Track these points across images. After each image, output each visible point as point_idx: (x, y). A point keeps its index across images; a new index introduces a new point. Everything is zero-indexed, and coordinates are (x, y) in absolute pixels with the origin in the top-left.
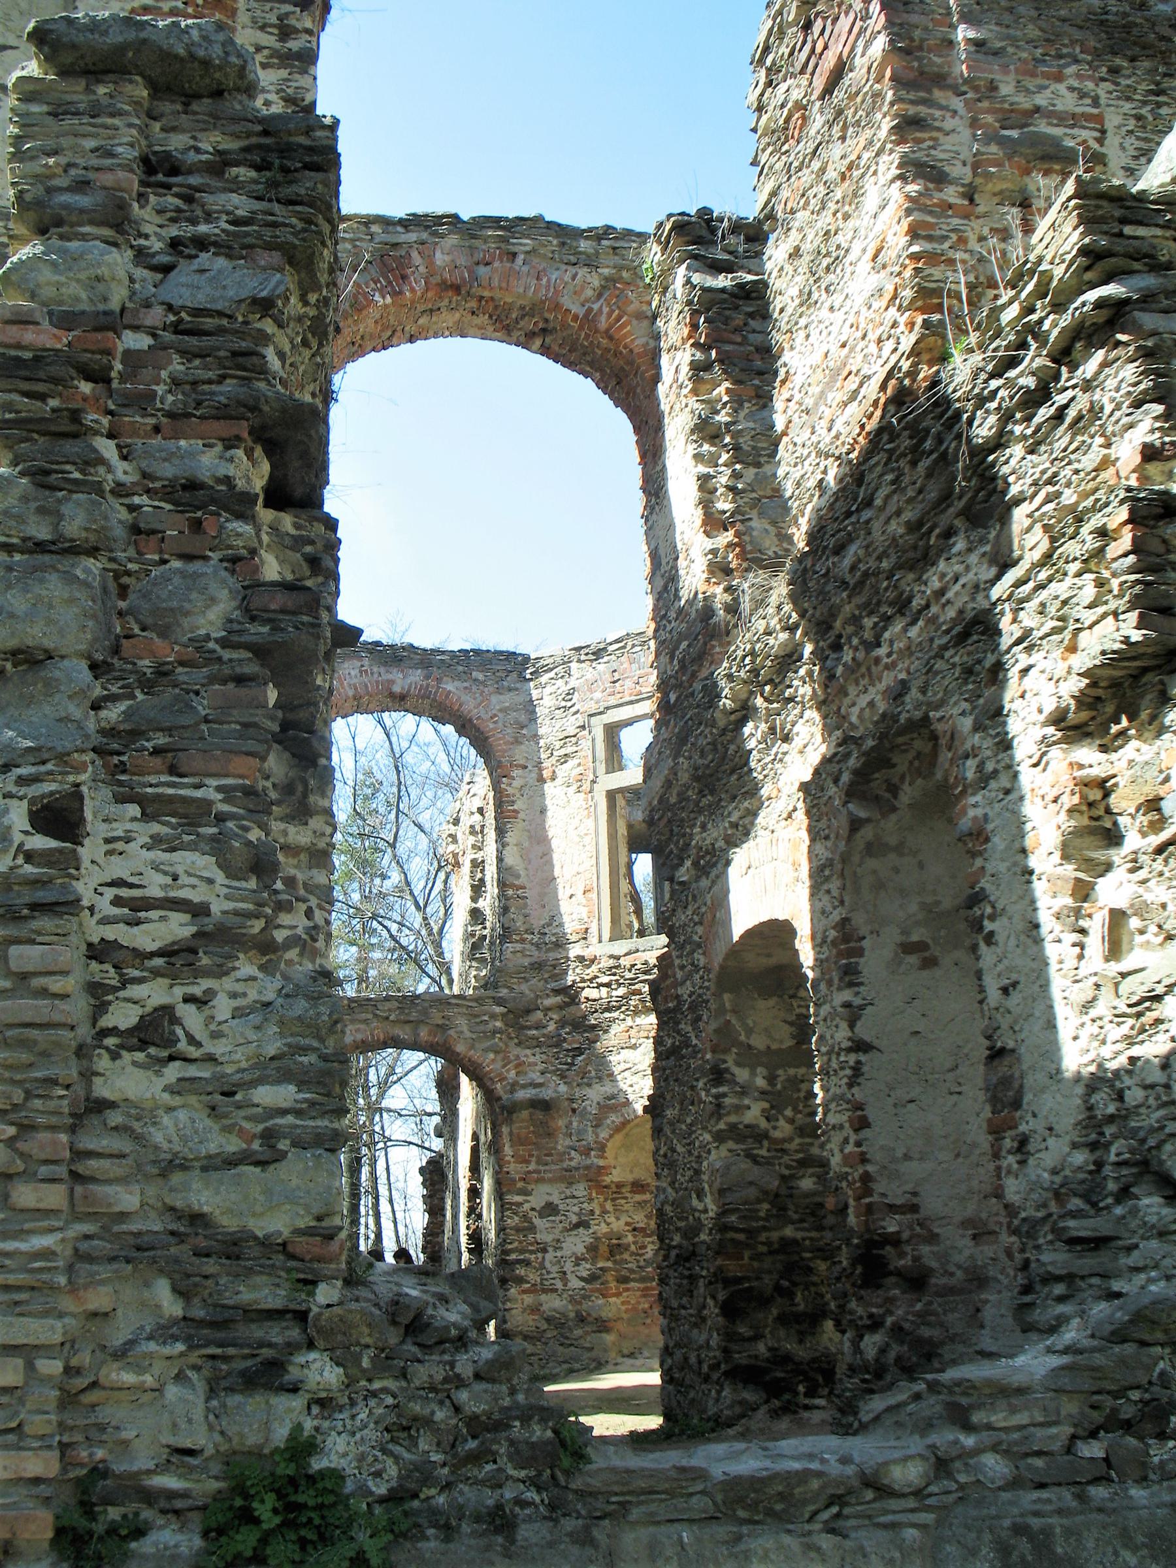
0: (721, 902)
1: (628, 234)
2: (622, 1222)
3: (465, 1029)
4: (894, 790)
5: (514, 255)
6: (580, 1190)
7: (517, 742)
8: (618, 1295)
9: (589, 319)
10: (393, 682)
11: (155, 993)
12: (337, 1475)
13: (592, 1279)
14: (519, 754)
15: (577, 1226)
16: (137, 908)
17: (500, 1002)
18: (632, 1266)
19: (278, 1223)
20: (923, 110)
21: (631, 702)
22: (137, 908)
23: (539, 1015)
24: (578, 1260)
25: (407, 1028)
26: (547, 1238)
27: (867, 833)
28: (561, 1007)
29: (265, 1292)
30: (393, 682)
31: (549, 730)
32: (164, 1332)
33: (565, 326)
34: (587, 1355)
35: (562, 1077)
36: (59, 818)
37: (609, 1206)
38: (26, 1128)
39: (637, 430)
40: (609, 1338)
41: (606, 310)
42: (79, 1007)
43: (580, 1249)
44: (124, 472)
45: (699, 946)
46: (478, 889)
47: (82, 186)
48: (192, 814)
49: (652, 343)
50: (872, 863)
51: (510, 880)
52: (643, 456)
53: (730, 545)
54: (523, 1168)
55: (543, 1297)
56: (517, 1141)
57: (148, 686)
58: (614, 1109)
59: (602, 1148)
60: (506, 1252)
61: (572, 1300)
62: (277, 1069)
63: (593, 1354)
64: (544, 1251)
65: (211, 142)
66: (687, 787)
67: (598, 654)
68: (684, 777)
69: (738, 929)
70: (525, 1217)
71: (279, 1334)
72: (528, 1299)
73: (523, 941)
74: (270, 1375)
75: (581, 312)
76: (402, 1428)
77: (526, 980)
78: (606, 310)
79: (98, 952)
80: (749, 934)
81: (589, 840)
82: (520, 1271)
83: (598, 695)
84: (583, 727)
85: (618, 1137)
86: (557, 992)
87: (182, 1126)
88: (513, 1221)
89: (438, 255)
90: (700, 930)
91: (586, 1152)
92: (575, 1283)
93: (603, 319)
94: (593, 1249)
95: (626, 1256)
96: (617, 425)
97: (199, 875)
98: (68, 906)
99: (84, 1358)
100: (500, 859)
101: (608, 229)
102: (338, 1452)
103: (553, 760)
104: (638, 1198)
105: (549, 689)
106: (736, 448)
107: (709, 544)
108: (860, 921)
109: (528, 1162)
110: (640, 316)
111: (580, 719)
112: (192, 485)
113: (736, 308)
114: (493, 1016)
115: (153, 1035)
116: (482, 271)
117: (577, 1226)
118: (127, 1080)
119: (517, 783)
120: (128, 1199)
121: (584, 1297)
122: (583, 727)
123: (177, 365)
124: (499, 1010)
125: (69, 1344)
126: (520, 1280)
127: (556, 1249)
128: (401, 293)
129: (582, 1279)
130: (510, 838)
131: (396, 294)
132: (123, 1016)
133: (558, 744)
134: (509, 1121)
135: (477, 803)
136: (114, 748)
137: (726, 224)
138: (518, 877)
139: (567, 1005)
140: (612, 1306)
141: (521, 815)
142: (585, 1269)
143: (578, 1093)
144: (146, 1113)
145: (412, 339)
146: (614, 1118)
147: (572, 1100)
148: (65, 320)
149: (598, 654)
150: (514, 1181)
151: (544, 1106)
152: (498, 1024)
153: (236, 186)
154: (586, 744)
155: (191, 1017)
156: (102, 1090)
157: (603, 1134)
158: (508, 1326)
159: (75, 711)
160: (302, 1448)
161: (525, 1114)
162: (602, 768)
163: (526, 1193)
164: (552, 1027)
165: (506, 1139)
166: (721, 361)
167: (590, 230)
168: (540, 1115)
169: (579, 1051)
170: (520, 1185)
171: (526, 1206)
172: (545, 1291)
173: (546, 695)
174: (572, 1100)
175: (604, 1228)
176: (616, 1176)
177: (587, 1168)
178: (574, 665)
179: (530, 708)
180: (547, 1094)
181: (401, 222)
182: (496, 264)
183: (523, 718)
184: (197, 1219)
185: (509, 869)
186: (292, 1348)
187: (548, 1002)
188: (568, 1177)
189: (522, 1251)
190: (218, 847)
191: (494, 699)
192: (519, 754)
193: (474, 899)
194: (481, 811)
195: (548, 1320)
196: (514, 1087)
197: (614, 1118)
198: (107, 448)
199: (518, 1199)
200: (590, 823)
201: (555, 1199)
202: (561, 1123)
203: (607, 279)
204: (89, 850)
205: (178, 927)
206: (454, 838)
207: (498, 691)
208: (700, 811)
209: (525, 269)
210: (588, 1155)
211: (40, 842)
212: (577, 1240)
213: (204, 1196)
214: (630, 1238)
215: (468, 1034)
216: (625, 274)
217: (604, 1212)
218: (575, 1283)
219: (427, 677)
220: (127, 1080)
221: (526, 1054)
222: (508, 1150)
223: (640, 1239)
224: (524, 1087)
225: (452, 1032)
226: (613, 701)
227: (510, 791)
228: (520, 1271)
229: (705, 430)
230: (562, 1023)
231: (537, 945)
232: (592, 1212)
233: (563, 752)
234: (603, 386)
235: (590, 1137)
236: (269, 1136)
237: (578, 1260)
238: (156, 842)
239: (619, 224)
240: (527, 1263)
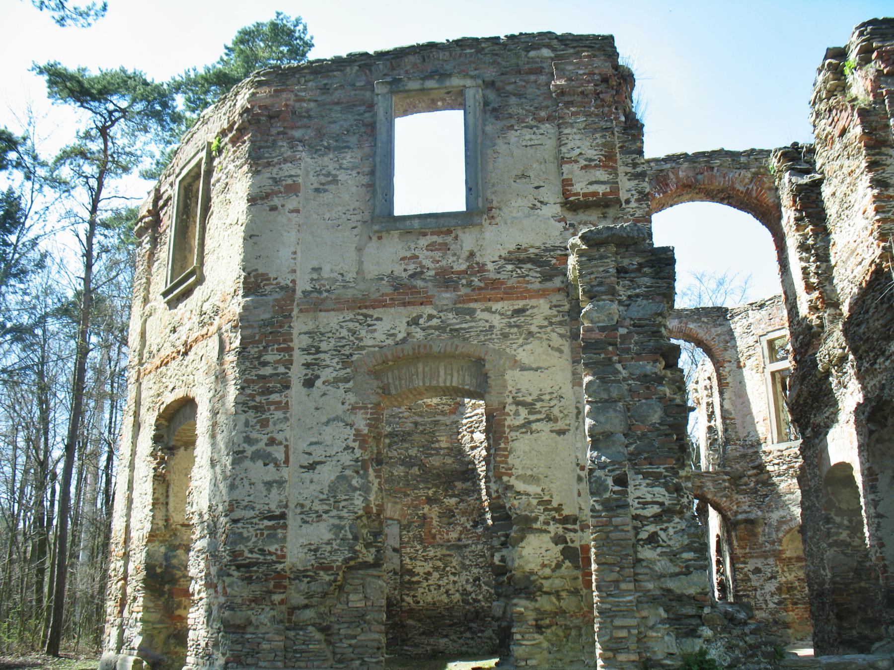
0: (825, 449)
1: (761, 151)
2: (793, 576)
4: (886, 419)
5: (713, 168)
6: (771, 561)
7: (726, 350)
8: (793, 611)
9: (748, 193)
11: (652, 528)
12: (714, 660)
13: (780, 603)
14: (727, 355)
15: (771, 578)
16: (644, 504)
17: (727, 474)
18: (799, 597)
19: (692, 591)
20: (878, 157)
21: (779, 329)
22: (644, 504)
23: (746, 479)
24: (772, 595)
26: (758, 584)
27: (876, 435)
28: (756, 475)
29: (689, 610)
31: (742, 344)
32: (663, 622)
33: (738, 196)
35: (759, 508)
36: (621, 481)
37: (786, 569)
38: (622, 568)
39: (774, 235)
40: (790, 631)
41: (755, 188)
42: (632, 534)
43: (773, 589)
44: (624, 373)
45: (816, 466)
46: (711, 416)
47: (601, 284)
48: (657, 476)
49: (777, 201)
50: (879, 446)
51: (728, 416)
52: (777, 247)
53: (817, 298)
54: (742, 551)
56: (739, 539)
57: (640, 439)
58: (785, 523)
59: (780, 541)
60: (738, 591)
61: (771, 613)
62: (688, 548)
64: (756, 590)
65: (636, 260)
66: (806, 398)
67: (761, 306)
68: (805, 394)
69: (832, 464)
70: (746, 575)
71: (694, 622)
73: (735, 444)
74: (693, 633)
75: (744, 190)
76: (730, 648)
77: (739, 463)
78: (755, 188)
79: (636, 517)
80: (835, 465)
81: (764, 395)
83: (763, 326)
84: (757, 342)
85: (788, 536)
86: (754, 468)
87: (663, 566)
88: (740, 576)
89: (680, 173)
90: (816, 460)
92: (771, 605)
93: (754, 192)
94: (779, 589)
95: (796, 592)
96: (765, 235)
97: (661, 494)
98: (626, 506)
99: (642, 629)
100: (722, 406)
101: (753, 150)
102: (713, 654)
103: (744, 358)
104: (800, 564)
105: (739, 324)
106: (817, 255)
107: (808, 297)
108: (876, 468)
110: (770, 189)
111: (755, 338)
112: (646, 376)
113: (812, 191)
114: (724, 481)
115: (653, 539)
116: (700, 177)
118: (647, 553)
119: (727, 370)
120: (650, 586)
122: (757, 342)
123: (636, 337)
124: (726, 477)
125: (638, 626)
128: (666, 192)
129: (775, 603)
130: (726, 396)
131: (664, 193)
132: (644, 535)
133: (745, 350)
134: (735, 530)
135: (707, 375)
136: (632, 459)
137: (805, 149)
139: (759, 474)
140: (791, 616)
142: (776, 599)
144: (653, 562)
145: (671, 206)
146: (785, 527)
148: (602, 329)
149: (761, 306)
150: (739, 558)
151: (751, 522)
152: (727, 484)
153: (645, 275)
154: (759, 350)
155: (662, 534)
156: (640, 556)
157: (781, 535)
159: (621, 449)
160: (703, 653)
161: (742, 526)
162: (767, 361)
163: (746, 563)
164: (752, 484)
165: (734, 538)
166: (807, 216)
167: (744, 152)
168: (749, 526)
169: (766, 496)
170: (742, 559)
171: (746, 569)
173: (738, 326)
174: (764, 519)
175: (784, 579)
176: (788, 554)
177: (774, 551)
178: (750, 312)
179: (731, 333)
180: (752, 516)
181: (663, 160)
182: (706, 173)
183: (728, 338)
184: (669, 591)
185: (726, 411)
186: (698, 625)
187: (750, 473)
188: (765, 555)
189: (745, 590)
190: (665, 486)
191: (713, 330)
192: (727, 355)
193: (709, 421)
194: (709, 378)
196: (736, 513)
197: (785, 527)
198: (619, 367)
199: (742, 566)
200: (764, 387)
201: (760, 566)
202: (760, 530)
203: (754, 174)
204: (630, 489)
205: (656, 509)
206: (696, 391)
207: (715, 326)
208: (813, 409)
209: (718, 174)
210: (774, 545)
211: (617, 488)
213: (671, 584)
214: (797, 584)
215: (713, 490)
216: (762, 170)
217: (783, 571)
219: (680, 323)
220: (647, 553)
221: (740, 498)
222: (735, 543)
223: (802, 584)
224: (741, 513)
225: (705, 489)
226: (770, 329)
227: (724, 373)
229: (803, 247)
230: (757, 483)
231: (743, 446)
232: (778, 572)
233: (748, 354)
234: (756, 216)
235: (774, 536)
236: (687, 567)
237: (772, 595)
238: (648, 485)
239: (758, 147)
240: (748, 596)
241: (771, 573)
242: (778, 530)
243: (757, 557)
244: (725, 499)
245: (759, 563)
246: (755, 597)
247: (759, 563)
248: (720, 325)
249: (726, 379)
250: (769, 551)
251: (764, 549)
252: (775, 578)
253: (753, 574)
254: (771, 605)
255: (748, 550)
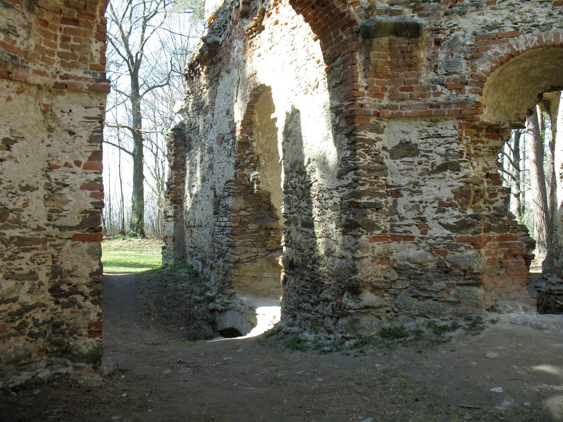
2: (480, 168)
6: (449, 128)
15: (442, 168)
24: (442, 207)
26: (404, 181)
34: (450, 309)
43: (446, 194)
55: (394, 245)
58: (498, 39)
61: (432, 249)
63: (461, 308)
64: (397, 194)
72: (379, 247)
82: (372, 216)
91: (459, 86)
109: (381, 96)
117: (442, 168)
121: (450, 247)
126: (372, 226)
127: (412, 193)
129: (447, 226)
142: (451, 216)
143: (444, 22)
147: (437, 31)
150: (368, 115)
151: (414, 31)
157: (482, 67)
158: (358, 276)
161: (384, 40)
163: (379, 130)
168: (402, 42)
170: (373, 120)
171: (379, 145)
172: (396, 238)
188: (434, 114)
189: (373, 194)
195: (399, 270)
197: (498, 50)
199: (371, 136)
201: (414, 138)
210: (460, 90)
212: (442, 184)
218: (436, 231)
228: (372, 216)
235: (464, 69)
237: (442, 207)
240: (377, 208)
241: (445, 156)
242: (474, 56)
243: (409, 117)
245: (413, 133)
246: (393, 211)
247: (413, 133)
250: (447, 104)
251: (431, 99)
252: (456, 168)
253: (393, 156)
254: (436, 231)
255: (385, 101)
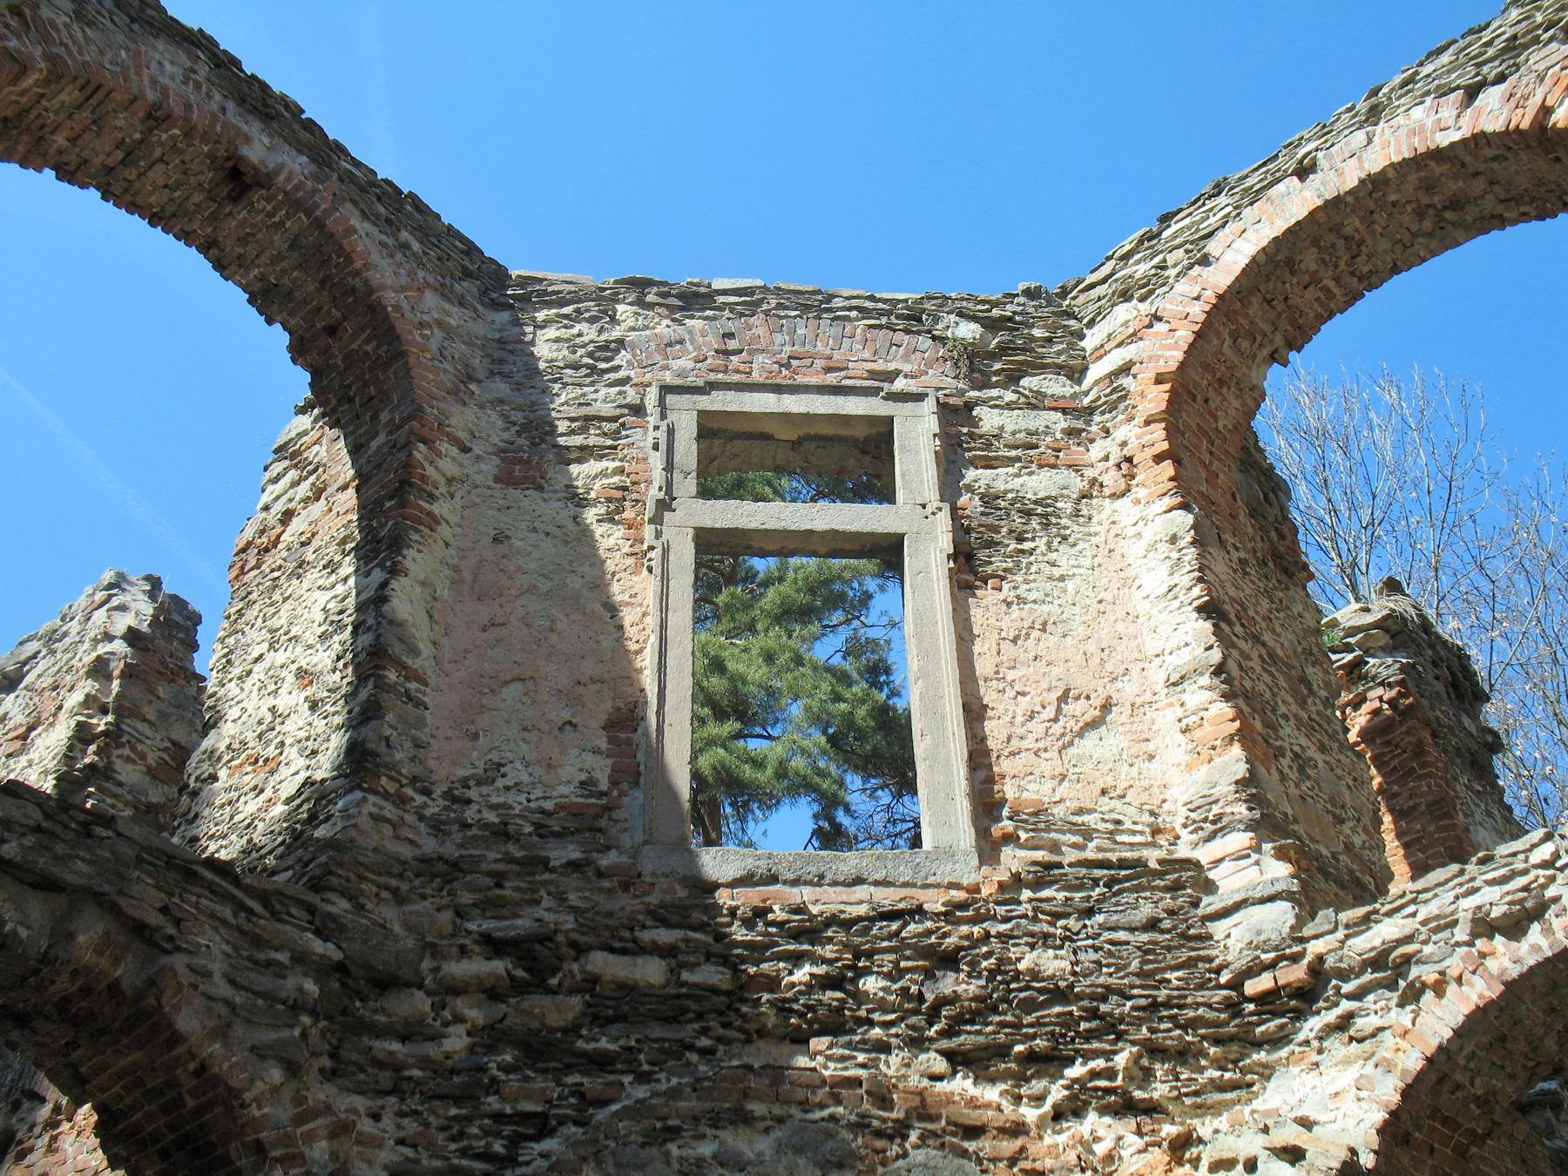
3: (217, 968)
10: (248, 139)
23: (420, 1002)
25: (38, 908)
28: (492, 993)
30: (248, 139)
51: (397, 649)
73: (401, 801)
77: (399, 898)
86: (494, 946)
114: (301, 958)
138: (415, 652)
139: (518, 988)
141: (444, 530)
149: (694, 300)
162: (687, 486)
164: (456, 1042)
169: (542, 1126)
187: (459, 969)
215: (223, 989)
219: (316, 178)
225: (179, 961)
230: (490, 1037)
231: (438, 827)
244: (276, 1075)
248: (461, 303)
249: (432, 498)
